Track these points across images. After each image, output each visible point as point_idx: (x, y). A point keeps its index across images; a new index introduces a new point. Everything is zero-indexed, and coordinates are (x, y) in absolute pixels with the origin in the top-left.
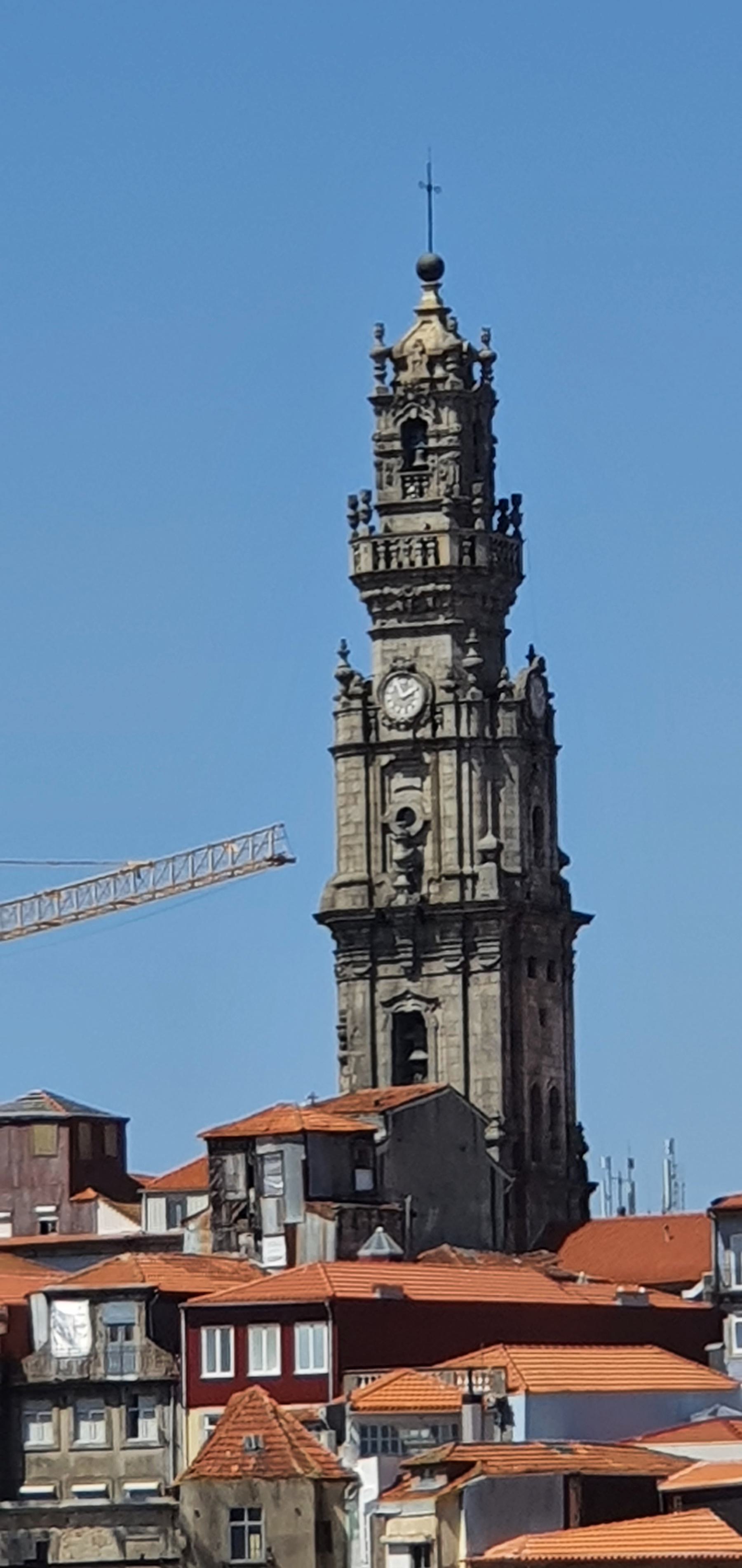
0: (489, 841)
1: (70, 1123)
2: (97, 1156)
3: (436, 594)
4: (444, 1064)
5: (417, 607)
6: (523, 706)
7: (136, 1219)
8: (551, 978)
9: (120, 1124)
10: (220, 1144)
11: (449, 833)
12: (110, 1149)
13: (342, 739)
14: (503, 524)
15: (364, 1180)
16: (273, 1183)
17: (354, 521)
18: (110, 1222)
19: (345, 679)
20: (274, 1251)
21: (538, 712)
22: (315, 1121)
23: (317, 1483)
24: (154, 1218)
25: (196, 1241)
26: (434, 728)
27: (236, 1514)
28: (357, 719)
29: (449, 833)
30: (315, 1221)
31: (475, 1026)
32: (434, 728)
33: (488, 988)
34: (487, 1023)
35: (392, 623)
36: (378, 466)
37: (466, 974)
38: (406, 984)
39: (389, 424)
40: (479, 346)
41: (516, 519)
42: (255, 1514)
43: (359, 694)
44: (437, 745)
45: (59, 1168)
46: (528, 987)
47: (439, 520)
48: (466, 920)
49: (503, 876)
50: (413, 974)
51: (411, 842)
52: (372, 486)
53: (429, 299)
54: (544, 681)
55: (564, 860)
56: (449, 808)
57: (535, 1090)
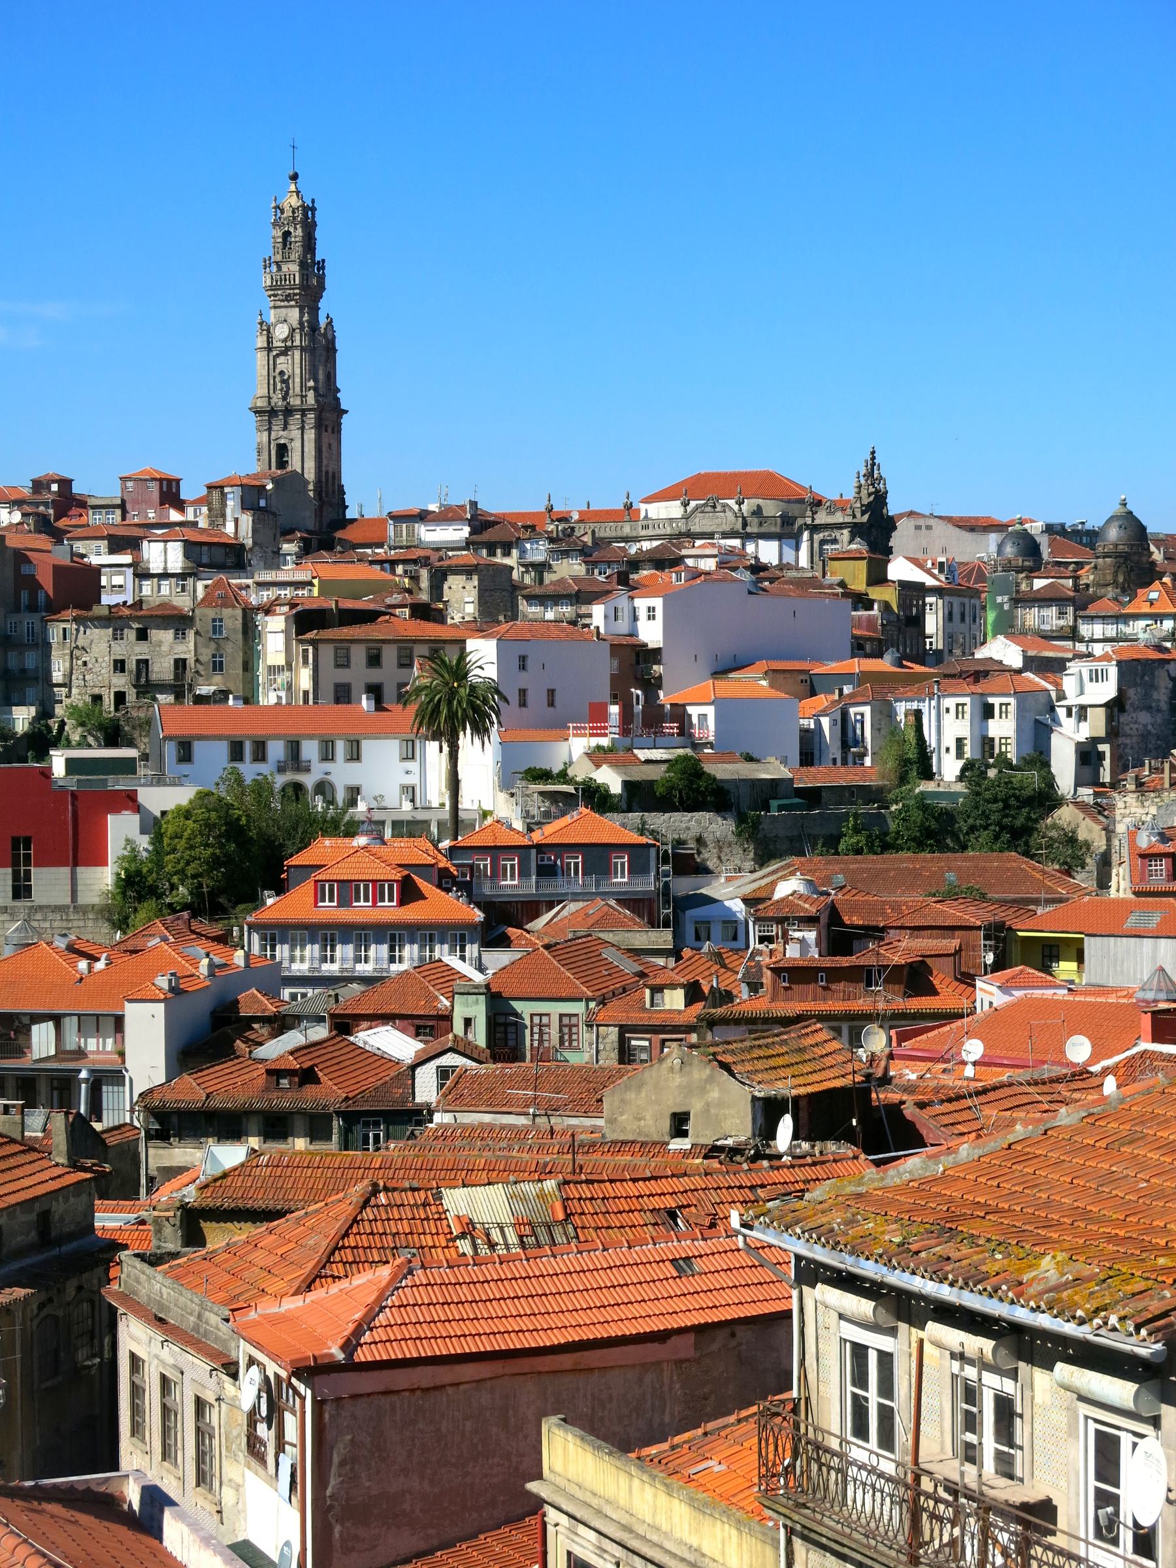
0: (311, 384)
1: (161, 480)
2: (170, 494)
3: (295, 294)
4: (295, 463)
5: (288, 298)
6: (325, 335)
8: (333, 432)
9: (178, 481)
10: (209, 487)
11: (298, 380)
13: (259, 345)
14: (319, 270)
15: (262, 503)
16: (230, 503)
18: (174, 516)
19: (261, 324)
21: (330, 337)
22: (245, 481)
23: (244, 610)
24: (190, 515)
25: (203, 523)
27: (214, 620)
28: (265, 338)
30: (244, 516)
31: (306, 449)
33: (310, 435)
34: (310, 448)
35: (279, 303)
37: (302, 429)
38: (282, 433)
39: (279, 233)
41: (323, 268)
42: (221, 620)
43: (267, 330)
45: (156, 495)
46: (324, 434)
47: (294, 268)
48: (303, 412)
49: (317, 395)
50: (285, 428)
51: (283, 381)
55: (338, 391)
56: (297, 371)
57: (327, 473)
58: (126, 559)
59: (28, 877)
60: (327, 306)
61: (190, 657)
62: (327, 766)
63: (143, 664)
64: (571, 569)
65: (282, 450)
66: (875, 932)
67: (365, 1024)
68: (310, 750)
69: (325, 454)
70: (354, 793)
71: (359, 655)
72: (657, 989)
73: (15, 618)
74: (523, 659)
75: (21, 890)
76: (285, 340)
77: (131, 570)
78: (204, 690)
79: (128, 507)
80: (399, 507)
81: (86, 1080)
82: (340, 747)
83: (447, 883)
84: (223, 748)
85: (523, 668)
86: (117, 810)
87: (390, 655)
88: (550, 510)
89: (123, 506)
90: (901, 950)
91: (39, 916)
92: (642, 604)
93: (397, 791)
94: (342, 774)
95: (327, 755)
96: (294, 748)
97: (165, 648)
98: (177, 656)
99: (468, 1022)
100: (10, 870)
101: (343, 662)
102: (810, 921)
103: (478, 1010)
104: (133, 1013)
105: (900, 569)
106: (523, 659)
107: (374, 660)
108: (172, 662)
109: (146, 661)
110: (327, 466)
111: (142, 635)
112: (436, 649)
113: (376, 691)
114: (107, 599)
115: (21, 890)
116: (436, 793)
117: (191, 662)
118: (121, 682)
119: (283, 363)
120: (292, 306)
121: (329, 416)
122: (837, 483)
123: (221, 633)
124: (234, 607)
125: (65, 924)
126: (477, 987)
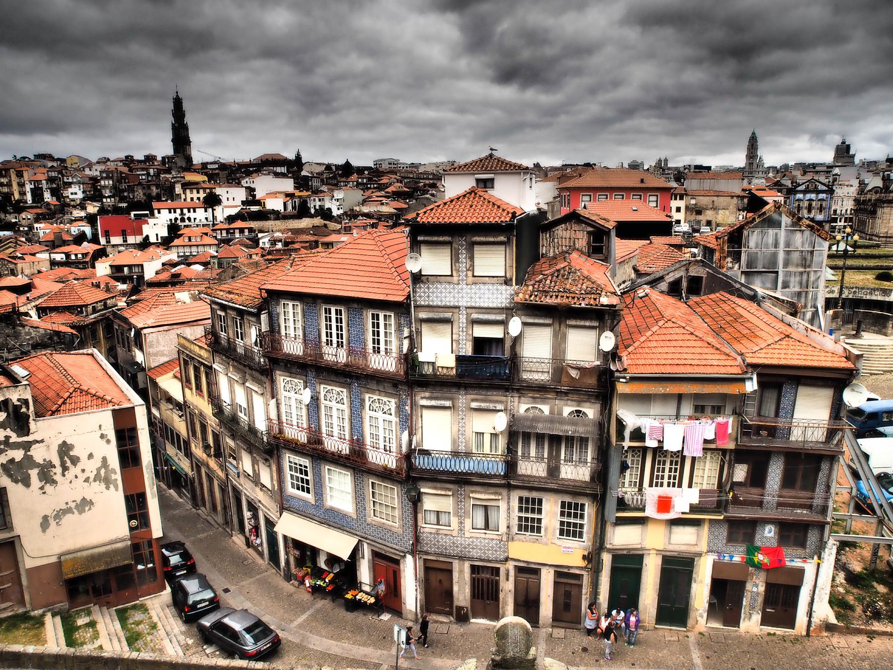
66: (293, 243)
68: (185, 211)
70: (195, 219)
71: (195, 191)
75: (125, 241)
80: (205, 161)
87: (201, 191)
90: (296, 246)
95: (189, 212)
96: (182, 210)
101: (192, 193)
102: (280, 241)
103: (216, 261)
104: (146, 265)
105: (304, 173)
107: (198, 192)
112: (211, 189)
113: (199, 199)
115: (125, 241)
116: (211, 218)
121: (188, 142)
122: (291, 156)
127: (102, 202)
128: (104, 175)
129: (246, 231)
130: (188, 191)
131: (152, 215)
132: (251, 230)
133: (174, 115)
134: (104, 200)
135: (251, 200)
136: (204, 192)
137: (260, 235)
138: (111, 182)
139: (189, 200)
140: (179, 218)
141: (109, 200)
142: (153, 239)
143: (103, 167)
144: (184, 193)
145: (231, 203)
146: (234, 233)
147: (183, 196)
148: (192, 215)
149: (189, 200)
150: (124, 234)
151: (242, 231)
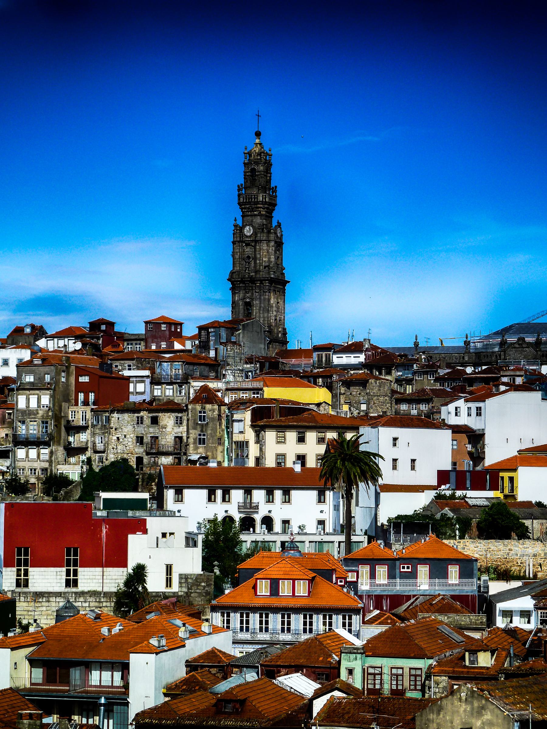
7: (184, 346)
9: (181, 324)
10: (201, 328)
12: (179, 330)
14: (273, 193)
17: (239, 190)
19: (236, 226)
20: (212, 354)
24: (188, 345)
26: (255, 238)
27: (200, 412)
29: (258, 262)
32: (255, 238)
36: (245, 178)
40: (268, 152)
43: (239, 230)
44: (256, 241)
51: (249, 263)
52: (243, 183)
53: (257, 141)
54: (281, 228)
58: (147, 373)
59: (75, 573)
60: (277, 216)
61: (184, 435)
62: (270, 506)
63: (155, 439)
64: (429, 383)
65: (248, 305)
67: (283, 671)
69: (274, 309)
71: (292, 436)
72: (474, 652)
73: (74, 408)
74: (395, 439)
75: (71, 582)
76: (250, 236)
77: (148, 381)
78: (195, 457)
79: (150, 340)
81: (104, 705)
82: (278, 494)
83: (341, 582)
84: (204, 493)
85: (395, 445)
86: (134, 533)
87: (311, 436)
88: (416, 344)
89: (145, 340)
91: (82, 599)
92: (473, 405)
93: (315, 523)
94: (278, 511)
95: (270, 499)
97: (169, 429)
98: (177, 435)
99: (351, 672)
100: (64, 569)
106: (395, 439)
107: (301, 440)
108: (173, 438)
109: (157, 437)
110: (276, 316)
111: (155, 421)
114: (133, 398)
115: (71, 582)
117: (185, 438)
118: (140, 450)
119: (248, 250)
120: (255, 215)
123: (204, 420)
124: (211, 403)
125: (97, 604)
126: (357, 649)
127: (15, 460)
128: (30, 379)
129: (454, 570)
130: (270, 436)
131: (159, 499)
132: (467, 566)
133: (247, 206)
134: (21, 453)
135: (472, 468)
136: (321, 441)
137: (496, 587)
138: (46, 400)
139: (270, 462)
140: (237, 516)
141: (33, 453)
142: (155, 583)
143: (26, 355)
144: (259, 440)
145: (403, 476)
146: (413, 575)
147: (253, 451)
148: (278, 511)
149: (270, 462)
150: (71, 560)
151: (439, 569)
